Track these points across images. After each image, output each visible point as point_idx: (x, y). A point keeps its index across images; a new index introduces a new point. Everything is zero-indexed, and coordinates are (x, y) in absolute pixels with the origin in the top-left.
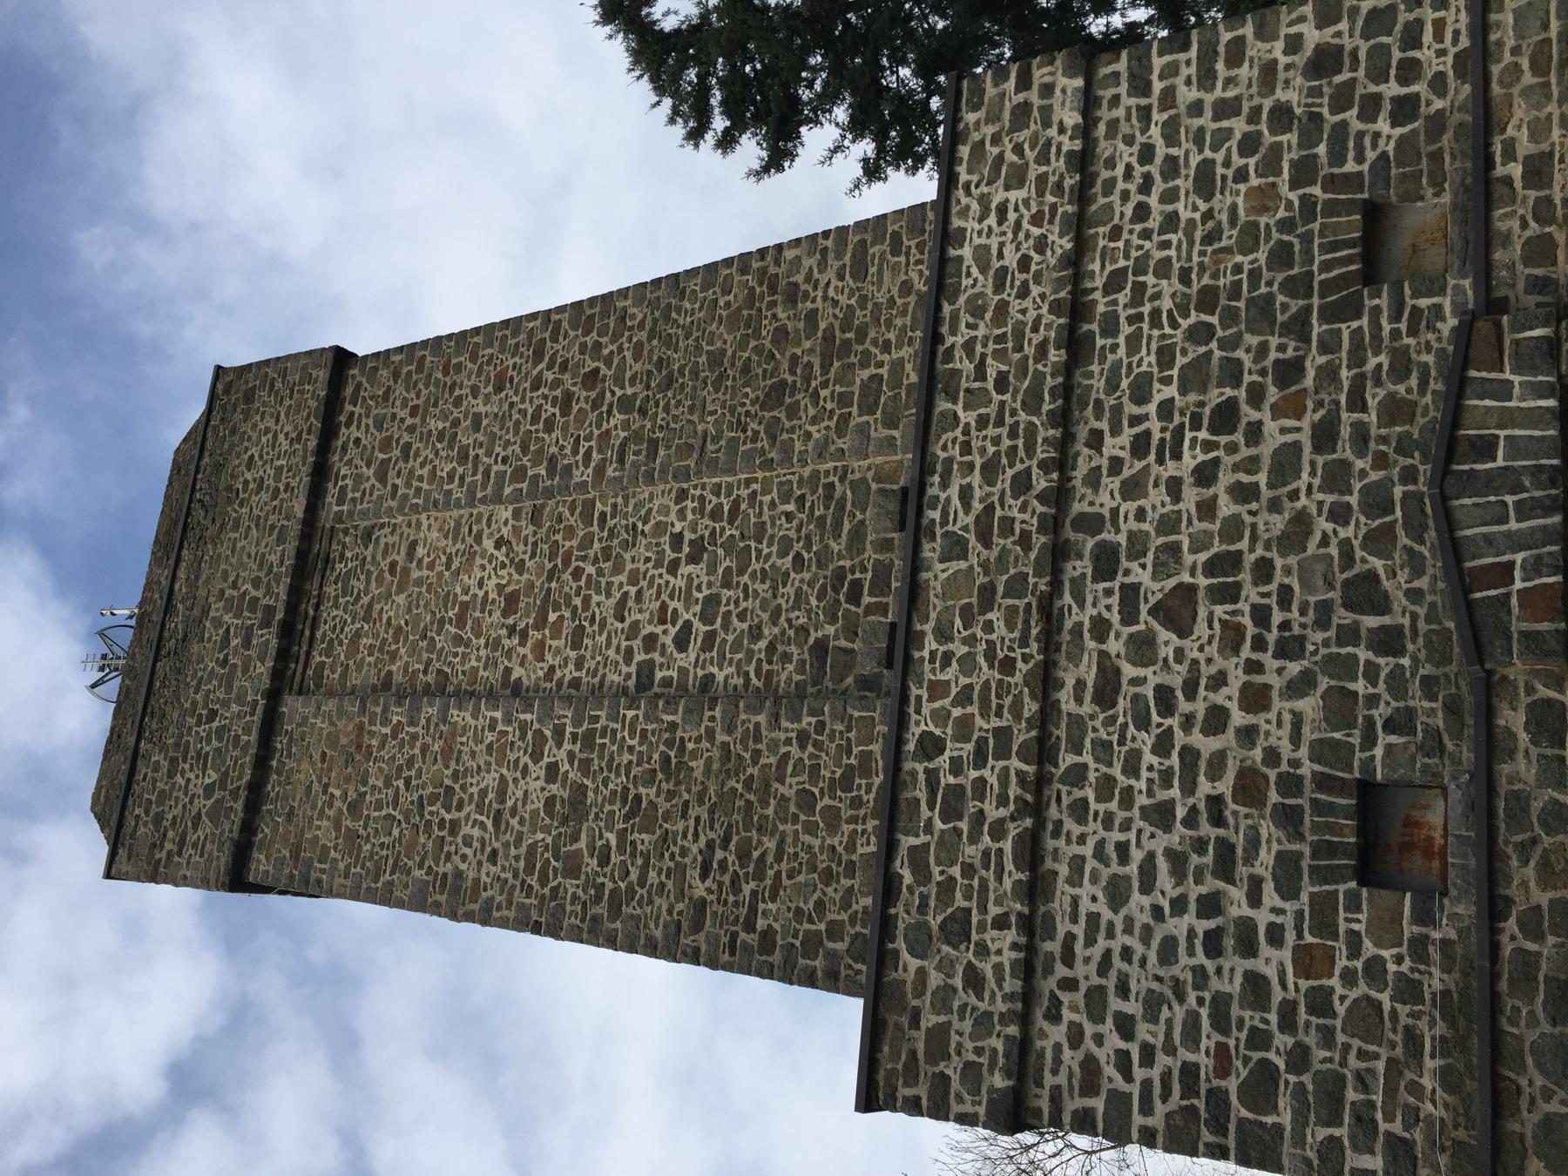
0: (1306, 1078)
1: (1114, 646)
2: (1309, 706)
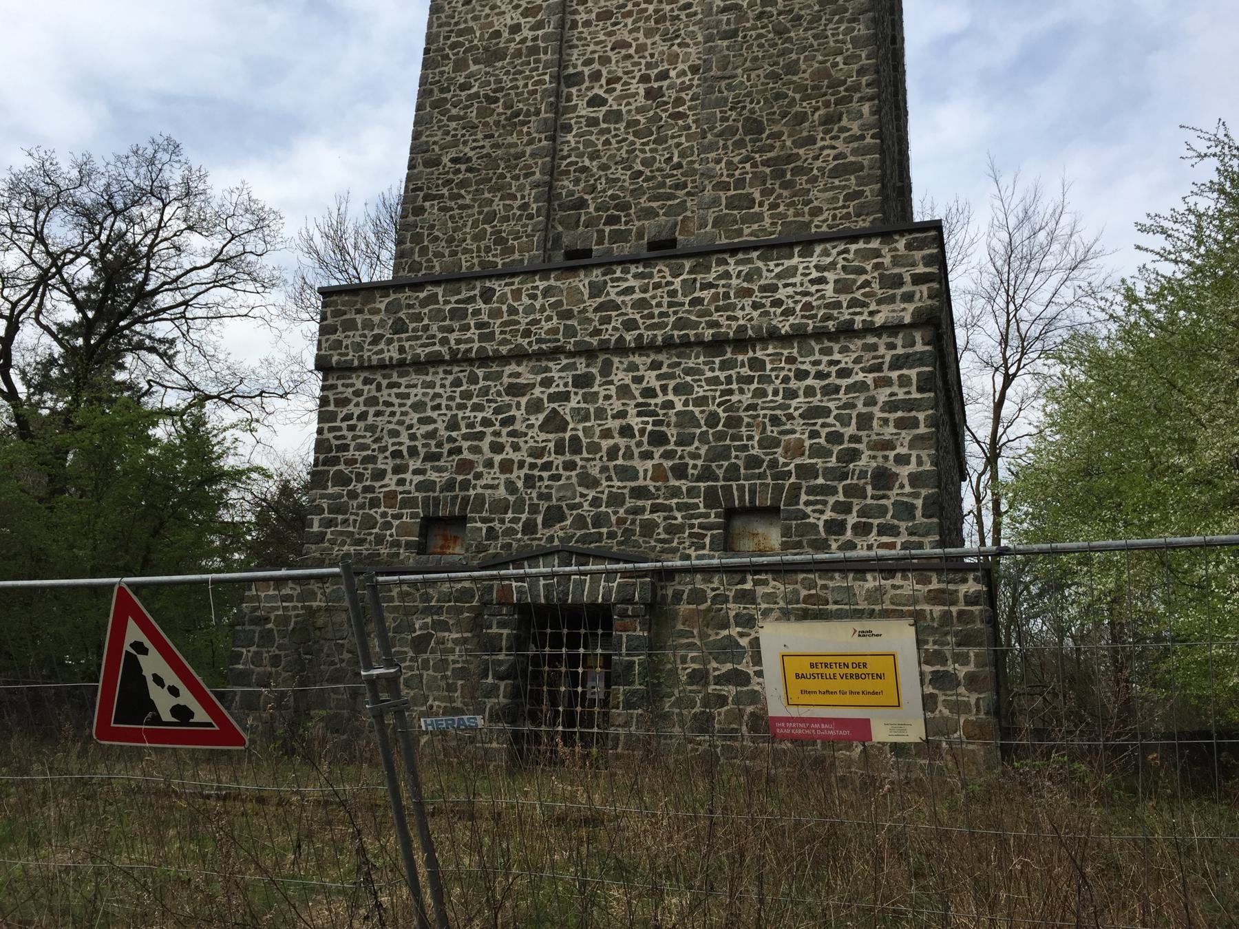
0: (346, 498)
1: (537, 391)
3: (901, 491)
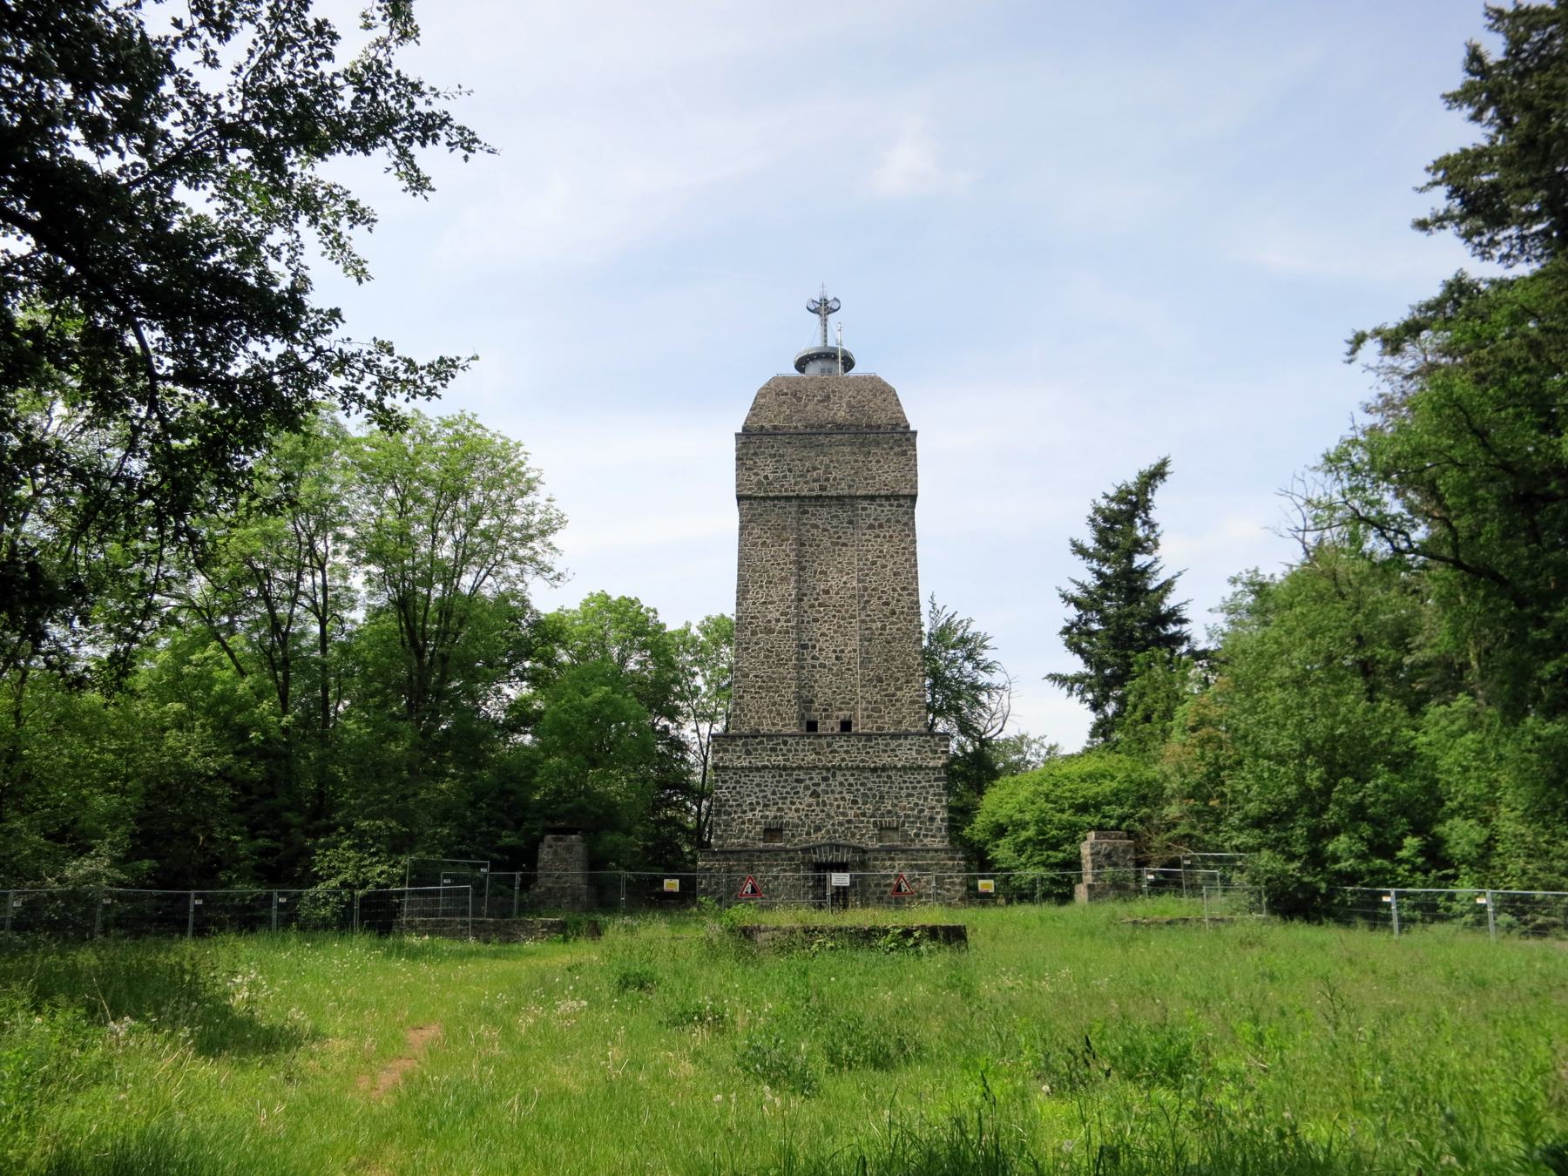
3: (938, 823)
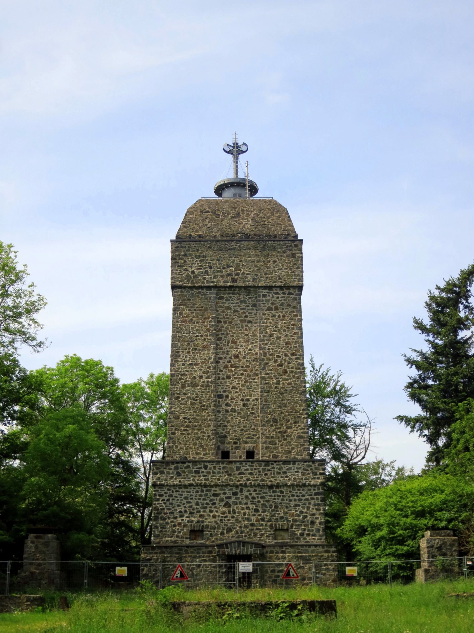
1: (222, 496)
2: (214, 524)
3: (317, 525)
